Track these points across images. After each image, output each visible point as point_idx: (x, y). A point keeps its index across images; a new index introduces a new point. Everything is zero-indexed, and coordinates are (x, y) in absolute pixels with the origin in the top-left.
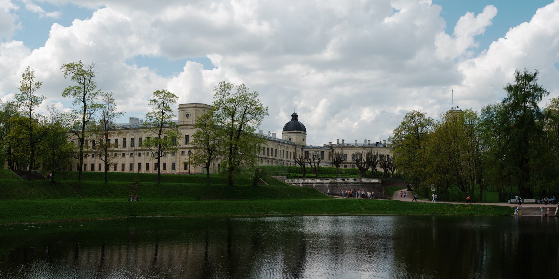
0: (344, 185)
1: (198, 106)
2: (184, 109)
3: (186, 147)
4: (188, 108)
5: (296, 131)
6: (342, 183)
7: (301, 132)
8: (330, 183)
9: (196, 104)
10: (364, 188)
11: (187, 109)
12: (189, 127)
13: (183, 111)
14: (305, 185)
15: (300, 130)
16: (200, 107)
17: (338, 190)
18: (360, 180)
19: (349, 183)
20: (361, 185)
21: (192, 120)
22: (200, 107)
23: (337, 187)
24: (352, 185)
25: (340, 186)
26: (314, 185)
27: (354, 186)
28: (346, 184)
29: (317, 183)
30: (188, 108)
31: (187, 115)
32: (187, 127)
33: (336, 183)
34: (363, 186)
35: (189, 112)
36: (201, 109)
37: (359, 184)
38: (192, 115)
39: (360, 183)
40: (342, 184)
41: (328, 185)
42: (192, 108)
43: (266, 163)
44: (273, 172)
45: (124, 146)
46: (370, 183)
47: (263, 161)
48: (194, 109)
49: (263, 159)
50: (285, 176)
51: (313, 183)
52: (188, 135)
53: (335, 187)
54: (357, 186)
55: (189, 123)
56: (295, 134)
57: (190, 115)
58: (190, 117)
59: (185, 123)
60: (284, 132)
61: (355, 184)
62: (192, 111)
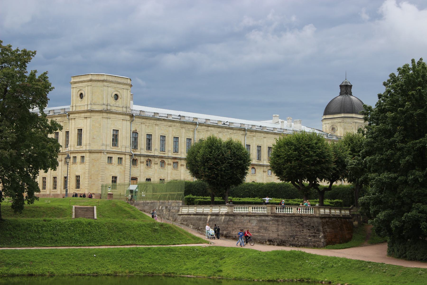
0: (246, 218)
2: (77, 84)
4: (82, 82)
5: (343, 115)
6: (242, 215)
7: (354, 115)
8: (227, 215)
10: (278, 225)
11: (80, 85)
12: (83, 115)
13: (75, 89)
14: (199, 217)
15: (352, 113)
16: (99, 81)
17: (235, 228)
18: (272, 209)
19: (254, 215)
20: (273, 220)
21: (86, 104)
22: (99, 81)
23: (235, 223)
24: (259, 218)
25: (238, 221)
26: (209, 217)
27: (260, 221)
28: (249, 218)
29: (212, 215)
30: (82, 82)
32: (80, 115)
33: (234, 215)
34: (277, 221)
35: (83, 89)
36: (101, 83)
37: (269, 218)
38: (86, 95)
39: (272, 216)
40: (242, 218)
41: (223, 217)
42: (86, 83)
43: (265, 174)
45: (149, 147)
46: (292, 216)
47: (257, 170)
48: (90, 83)
49: (255, 167)
50: (181, 201)
51: (206, 215)
52: (81, 129)
53: (232, 223)
54: (264, 221)
55: (83, 109)
56: (340, 120)
57: (84, 96)
58: (85, 98)
59: (78, 109)
60: (324, 117)
61: (263, 218)
62: (87, 87)
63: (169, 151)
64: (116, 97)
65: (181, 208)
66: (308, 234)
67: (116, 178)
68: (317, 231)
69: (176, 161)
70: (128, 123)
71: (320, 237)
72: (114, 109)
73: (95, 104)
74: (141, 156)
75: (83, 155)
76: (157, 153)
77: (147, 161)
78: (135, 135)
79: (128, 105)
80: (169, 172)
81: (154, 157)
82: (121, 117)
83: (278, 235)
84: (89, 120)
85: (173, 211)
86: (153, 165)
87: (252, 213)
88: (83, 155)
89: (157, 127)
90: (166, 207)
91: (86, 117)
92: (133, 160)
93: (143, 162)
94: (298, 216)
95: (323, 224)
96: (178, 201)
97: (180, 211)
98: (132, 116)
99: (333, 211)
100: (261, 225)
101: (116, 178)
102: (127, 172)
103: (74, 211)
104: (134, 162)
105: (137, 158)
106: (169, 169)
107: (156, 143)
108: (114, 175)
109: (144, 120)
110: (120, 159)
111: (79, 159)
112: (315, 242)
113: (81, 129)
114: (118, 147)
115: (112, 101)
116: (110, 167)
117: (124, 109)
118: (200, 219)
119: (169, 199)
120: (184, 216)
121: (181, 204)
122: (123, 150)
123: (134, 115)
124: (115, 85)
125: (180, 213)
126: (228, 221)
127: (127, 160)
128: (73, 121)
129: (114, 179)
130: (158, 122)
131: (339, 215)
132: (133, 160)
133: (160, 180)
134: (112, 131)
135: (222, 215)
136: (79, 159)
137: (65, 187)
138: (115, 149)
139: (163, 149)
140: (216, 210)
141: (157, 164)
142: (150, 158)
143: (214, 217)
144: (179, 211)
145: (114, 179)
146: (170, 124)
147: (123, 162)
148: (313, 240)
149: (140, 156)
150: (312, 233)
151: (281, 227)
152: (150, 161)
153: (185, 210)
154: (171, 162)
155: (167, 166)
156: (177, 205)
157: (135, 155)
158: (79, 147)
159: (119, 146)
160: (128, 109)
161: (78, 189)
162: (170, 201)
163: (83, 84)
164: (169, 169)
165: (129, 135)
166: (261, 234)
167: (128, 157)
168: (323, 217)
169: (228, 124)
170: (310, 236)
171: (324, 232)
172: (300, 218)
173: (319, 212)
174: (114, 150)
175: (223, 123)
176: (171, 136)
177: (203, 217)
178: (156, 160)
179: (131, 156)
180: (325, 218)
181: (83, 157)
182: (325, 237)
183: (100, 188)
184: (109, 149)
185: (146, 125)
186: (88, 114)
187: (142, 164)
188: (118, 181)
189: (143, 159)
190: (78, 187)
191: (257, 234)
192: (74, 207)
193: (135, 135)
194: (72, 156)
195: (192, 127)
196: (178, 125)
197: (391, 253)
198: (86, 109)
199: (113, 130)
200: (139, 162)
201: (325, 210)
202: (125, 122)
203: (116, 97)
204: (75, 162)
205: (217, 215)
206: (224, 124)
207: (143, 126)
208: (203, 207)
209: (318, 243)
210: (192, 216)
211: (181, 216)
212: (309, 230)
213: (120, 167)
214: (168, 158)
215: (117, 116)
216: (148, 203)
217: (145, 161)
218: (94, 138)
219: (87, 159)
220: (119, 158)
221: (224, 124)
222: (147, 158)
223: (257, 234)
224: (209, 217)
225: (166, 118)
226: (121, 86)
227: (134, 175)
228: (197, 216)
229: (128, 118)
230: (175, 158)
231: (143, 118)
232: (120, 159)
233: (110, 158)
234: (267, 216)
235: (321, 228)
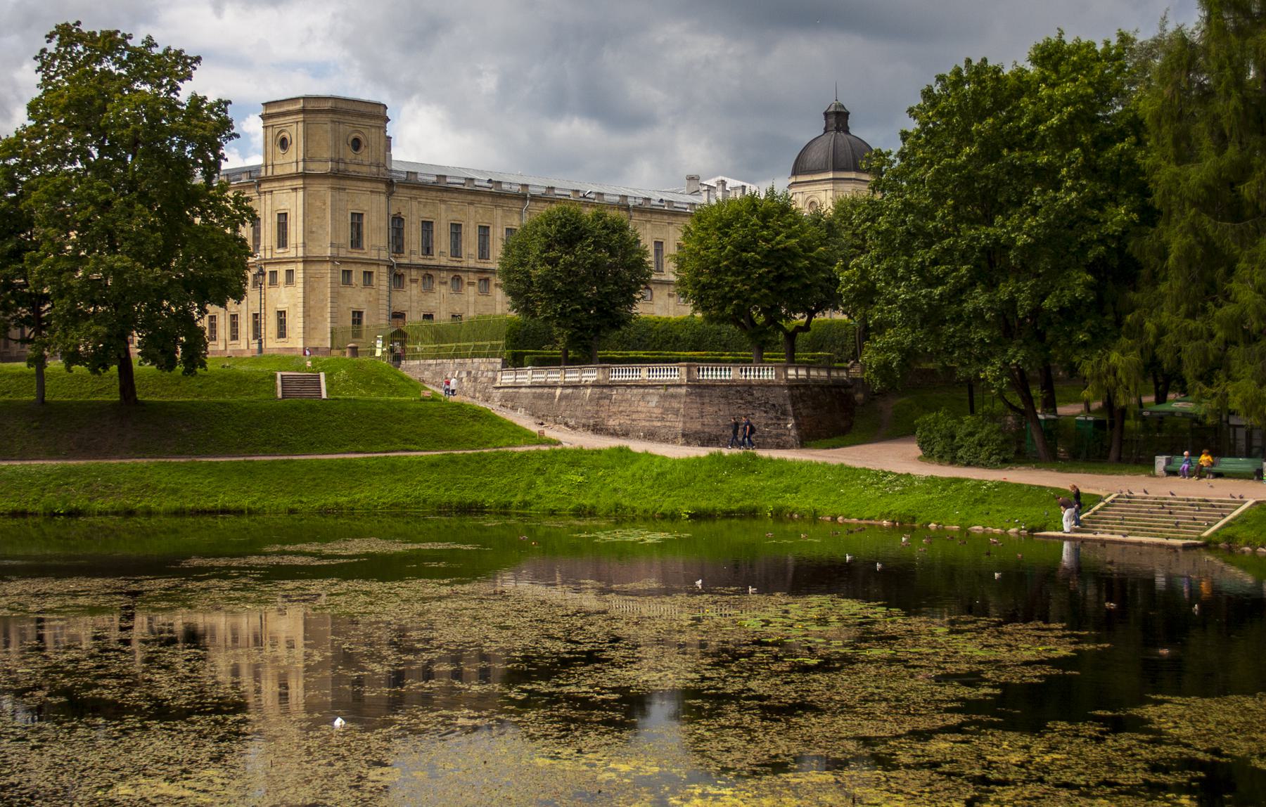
0: (635, 391)
1: (310, 106)
3: (281, 256)
5: (830, 175)
9: (304, 98)
11: (281, 120)
12: (288, 183)
14: (539, 391)
18: (689, 372)
21: (295, 160)
24: (662, 391)
28: (642, 390)
31: (284, 144)
33: (612, 386)
34: (701, 396)
37: (683, 391)
38: (294, 141)
40: (628, 391)
41: (589, 391)
43: (672, 301)
44: (461, 344)
46: (730, 386)
47: (656, 293)
48: (300, 117)
50: (499, 360)
51: (554, 386)
52: (286, 214)
53: (607, 402)
54: (673, 396)
58: (292, 148)
59: (278, 172)
60: (793, 180)
62: (295, 125)
63: (469, 256)
64: (356, 144)
65: (499, 374)
66: (764, 422)
68: (782, 414)
69: (484, 276)
70: (383, 198)
71: (789, 426)
73: (312, 160)
74: (410, 268)
75: (290, 267)
76: (444, 261)
77: (424, 278)
78: (397, 223)
79: (382, 161)
80: (472, 299)
81: (439, 268)
82: (368, 185)
83: (703, 425)
85: (484, 380)
86: (436, 286)
87: (649, 381)
88: (290, 267)
89: (443, 206)
90: (469, 373)
91: (296, 189)
92: (396, 275)
93: (416, 281)
94: (744, 385)
95: (795, 400)
96: (493, 360)
97: (499, 380)
98: (390, 183)
99: (813, 373)
100: (667, 405)
101: (360, 314)
102: (384, 302)
103: (279, 382)
104: (397, 278)
105: (402, 271)
106: (471, 293)
107: (442, 241)
108: (355, 307)
109: (414, 192)
110: (368, 275)
111: (281, 277)
112: (778, 436)
113: (286, 214)
114: (363, 249)
115: (349, 154)
116: (348, 291)
117: (374, 169)
118: (540, 396)
119: (474, 356)
120: (506, 390)
121: (499, 366)
122: (373, 255)
123: (395, 180)
125: (498, 385)
126: (599, 398)
127: (382, 278)
128: (268, 196)
129: (357, 316)
130: (446, 196)
131: (826, 382)
132: (396, 275)
133: (453, 316)
134: (350, 215)
135: (585, 386)
136: (281, 277)
137: (257, 333)
139: (456, 252)
140: (573, 376)
141: (446, 283)
143: (569, 391)
144: (495, 379)
145: (357, 316)
146: (470, 198)
147: (375, 281)
148: (774, 432)
149: (410, 266)
150: (772, 419)
151: (709, 409)
152: (430, 277)
153: (507, 378)
154: (473, 278)
155: (465, 286)
156: (490, 367)
157: (399, 265)
159: (365, 247)
160: (382, 169)
161: (282, 340)
162: (476, 360)
164: (471, 293)
165: (383, 224)
166: (668, 424)
167: (384, 269)
168: (794, 386)
169: (593, 196)
170: (767, 425)
171: (796, 417)
172: (746, 388)
173: (786, 374)
174: (355, 255)
175: (581, 195)
176: (472, 223)
177: (546, 390)
178: (444, 274)
179: (390, 267)
180: (797, 386)
181: (290, 273)
182: (797, 426)
183: (329, 335)
184: (343, 253)
185: (419, 202)
186: (299, 183)
187: (414, 285)
188: (365, 321)
189: (414, 274)
190: (282, 333)
191: (659, 424)
192: (279, 375)
193: (397, 223)
194: (268, 269)
195: (519, 204)
196: (487, 200)
197: (929, 455)
198: (294, 170)
199: (352, 214)
200: (407, 279)
201: (797, 372)
202: (375, 197)
204: (273, 282)
205: (575, 386)
206: (584, 196)
207: (414, 203)
208: (546, 372)
209: (784, 438)
210: (523, 390)
211: (501, 390)
212: (765, 412)
213: (368, 290)
214: (468, 270)
215: (359, 184)
216: (430, 365)
217: (420, 278)
218: (312, 232)
219: (299, 276)
220: (365, 272)
221: (584, 196)
222: (424, 272)
223: (659, 424)
224: (558, 391)
225: (461, 187)
227: (398, 309)
228: (533, 390)
229: (382, 187)
230: (484, 271)
231: (414, 188)
232: (368, 275)
233: (347, 274)
234: (680, 386)
235: (789, 408)
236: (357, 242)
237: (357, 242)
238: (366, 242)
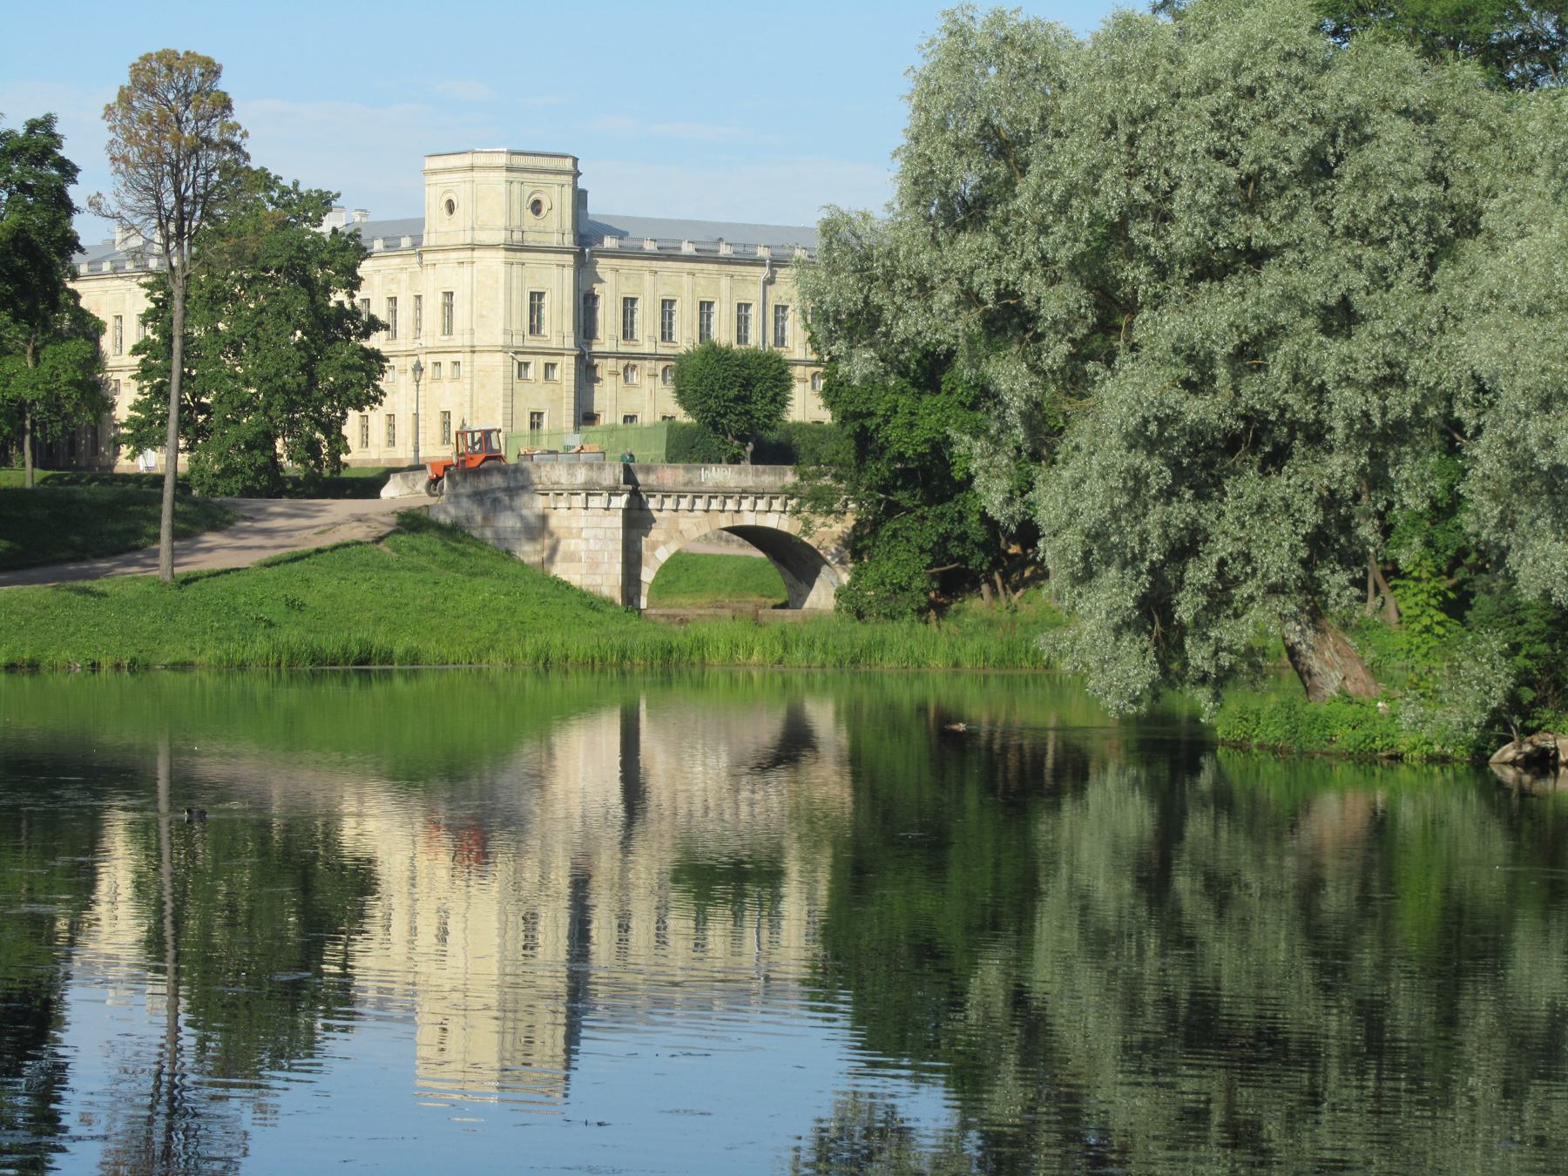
12: (454, 255)
52: (452, 293)
67: (540, 415)
72: (531, 239)
73: (482, 228)
74: (606, 358)
84: (467, 268)
101: (540, 415)
110: (550, 367)
122: (555, 343)
124: (536, 176)
128: (430, 270)
129: (536, 419)
138: (533, 342)
142: (632, 362)
145: (536, 419)
158: (446, 338)
163: (454, 176)
174: (535, 344)
184: (517, 341)
203: (536, 207)
218: (482, 316)
226: (550, 177)
233: (524, 366)
236: (535, 329)
237: (535, 329)
238: (545, 330)
